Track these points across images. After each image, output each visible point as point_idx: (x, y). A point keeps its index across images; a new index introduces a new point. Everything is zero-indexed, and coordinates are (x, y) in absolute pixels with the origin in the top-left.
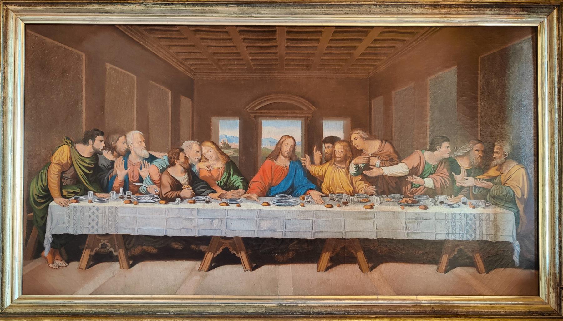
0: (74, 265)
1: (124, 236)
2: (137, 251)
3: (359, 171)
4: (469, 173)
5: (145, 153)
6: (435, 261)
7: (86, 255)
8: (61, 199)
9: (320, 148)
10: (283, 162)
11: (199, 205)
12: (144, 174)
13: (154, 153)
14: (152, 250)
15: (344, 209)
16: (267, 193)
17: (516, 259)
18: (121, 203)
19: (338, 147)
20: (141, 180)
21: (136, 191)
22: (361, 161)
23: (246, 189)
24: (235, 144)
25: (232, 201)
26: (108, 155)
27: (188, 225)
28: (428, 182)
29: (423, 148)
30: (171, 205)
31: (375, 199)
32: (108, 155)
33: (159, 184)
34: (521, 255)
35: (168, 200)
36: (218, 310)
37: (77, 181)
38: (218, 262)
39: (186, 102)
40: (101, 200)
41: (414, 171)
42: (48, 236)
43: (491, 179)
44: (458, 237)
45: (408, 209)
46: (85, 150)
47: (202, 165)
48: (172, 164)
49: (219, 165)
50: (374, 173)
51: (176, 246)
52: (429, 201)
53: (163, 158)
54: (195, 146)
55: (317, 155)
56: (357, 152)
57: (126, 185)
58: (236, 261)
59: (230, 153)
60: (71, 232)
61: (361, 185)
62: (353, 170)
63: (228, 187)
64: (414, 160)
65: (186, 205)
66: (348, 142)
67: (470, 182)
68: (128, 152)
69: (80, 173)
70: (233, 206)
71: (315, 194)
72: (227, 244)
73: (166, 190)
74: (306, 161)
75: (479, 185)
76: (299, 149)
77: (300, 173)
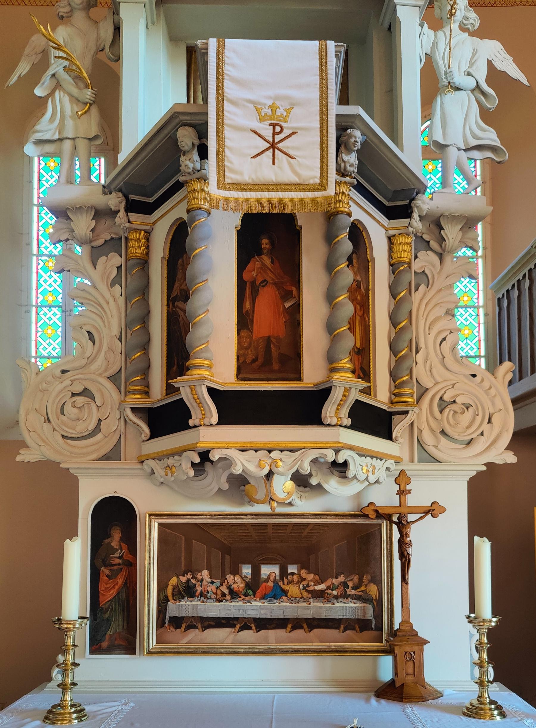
0: (178, 630)
1: (200, 617)
2: (206, 624)
3: (304, 588)
4: (353, 588)
5: (209, 580)
6: (338, 628)
7: (184, 626)
8: (173, 601)
9: (287, 578)
10: (270, 584)
11: (233, 603)
12: (209, 590)
13: (213, 580)
14: (213, 623)
15: (298, 605)
16: (263, 598)
17: (373, 627)
18: (199, 603)
19: (295, 577)
20: (208, 592)
21: (206, 597)
22: (305, 583)
23: (254, 596)
24: (250, 576)
25: (248, 601)
26: (194, 581)
27: (229, 612)
28: (335, 592)
29: (332, 578)
30: (221, 603)
31: (311, 600)
32: (194, 581)
33: (216, 594)
34: (375, 625)
35: (220, 601)
36: (242, 650)
37: (180, 593)
38: (242, 629)
39: (227, 557)
40: (190, 601)
41: (328, 588)
42: (167, 617)
43: (362, 591)
44: (348, 617)
45: (326, 605)
46: (183, 579)
47: (235, 585)
48: (222, 585)
49: (243, 585)
50: (311, 588)
51: (223, 622)
52: (335, 601)
53: (217, 582)
54: (232, 577)
55: (286, 581)
56: (303, 579)
57: (202, 594)
58: (251, 628)
59: (247, 580)
60: (177, 616)
61: (305, 594)
62: (301, 587)
63: (246, 595)
64: (328, 583)
65: (228, 603)
66: (299, 574)
67: (353, 592)
68: (202, 580)
69: (181, 589)
70: (248, 604)
71: (285, 598)
72: (246, 621)
73: (219, 596)
74: (281, 583)
75: (357, 594)
76: (278, 578)
77: (278, 589)
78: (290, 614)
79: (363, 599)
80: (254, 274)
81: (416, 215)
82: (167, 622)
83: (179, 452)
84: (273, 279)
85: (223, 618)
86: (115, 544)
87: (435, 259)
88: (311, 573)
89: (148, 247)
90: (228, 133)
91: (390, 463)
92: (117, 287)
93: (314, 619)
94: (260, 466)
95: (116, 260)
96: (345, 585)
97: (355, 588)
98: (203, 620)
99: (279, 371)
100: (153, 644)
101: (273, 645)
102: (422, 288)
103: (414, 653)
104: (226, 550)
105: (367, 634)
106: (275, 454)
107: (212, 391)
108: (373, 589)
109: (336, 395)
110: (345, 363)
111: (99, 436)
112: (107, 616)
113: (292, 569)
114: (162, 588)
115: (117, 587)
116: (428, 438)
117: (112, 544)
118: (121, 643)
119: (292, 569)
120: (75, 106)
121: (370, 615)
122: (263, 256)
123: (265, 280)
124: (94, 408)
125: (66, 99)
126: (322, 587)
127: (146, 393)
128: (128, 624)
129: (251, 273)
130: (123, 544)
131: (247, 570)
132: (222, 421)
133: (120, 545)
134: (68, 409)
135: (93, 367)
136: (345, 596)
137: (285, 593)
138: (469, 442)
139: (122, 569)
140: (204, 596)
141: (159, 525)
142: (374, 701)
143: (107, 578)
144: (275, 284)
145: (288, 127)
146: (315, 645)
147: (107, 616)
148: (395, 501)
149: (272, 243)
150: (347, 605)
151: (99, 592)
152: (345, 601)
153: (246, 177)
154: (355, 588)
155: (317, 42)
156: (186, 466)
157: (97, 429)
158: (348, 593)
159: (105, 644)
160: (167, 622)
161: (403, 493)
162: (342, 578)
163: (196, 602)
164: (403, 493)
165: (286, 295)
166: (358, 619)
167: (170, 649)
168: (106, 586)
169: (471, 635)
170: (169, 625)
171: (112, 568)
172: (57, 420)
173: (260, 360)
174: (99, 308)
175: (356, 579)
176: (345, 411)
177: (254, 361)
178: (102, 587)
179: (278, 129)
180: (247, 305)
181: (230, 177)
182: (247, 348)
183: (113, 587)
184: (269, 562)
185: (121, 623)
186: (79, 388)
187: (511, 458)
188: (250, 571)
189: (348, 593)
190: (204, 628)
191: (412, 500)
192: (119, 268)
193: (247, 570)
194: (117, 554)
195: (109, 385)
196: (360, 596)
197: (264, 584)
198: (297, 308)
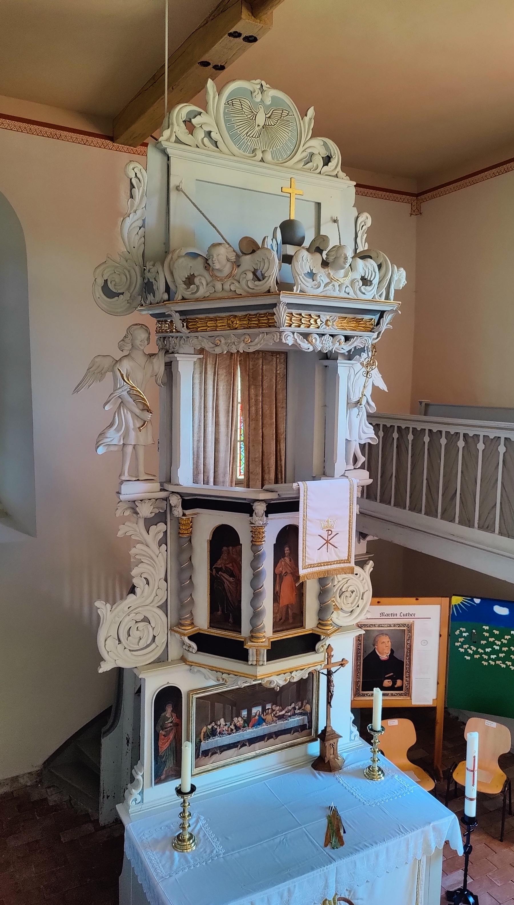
0: (207, 757)
1: (219, 746)
2: (222, 749)
3: (274, 715)
4: (298, 709)
5: (224, 724)
6: (290, 733)
7: (210, 754)
8: (204, 741)
9: (265, 712)
10: (257, 717)
11: (237, 734)
12: (224, 729)
13: (227, 723)
14: (226, 748)
15: (271, 725)
16: (253, 726)
17: (307, 727)
18: (219, 738)
19: (270, 710)
20: (223, 731)
21: (223, 734)
22: (274, 713)
23: (248, 727)
24: (246, 716)
25: (245, 730)
26: (216, 727)
27: (234, 739)
28: (289, 714)
29: (288, 706)
30: (231, 735)
31: (278, 721)
32: (216, 727)
33: (228, 731)
34: (308, 726)
35: (230, 734)
37: (208, 735)
38: (241, 747)
39: (234, 708)
40: (214, 739)
41: (286, 712)
42: (201, 751)
43: (303, 710)
44: (295, 726)
45: (285, 722)
46: (210, 727)
47: (238, 723)
48: (231, 725)
49: (242, 722)
50: (278, 715)
51: (231, 745)
52: (290, 718)
53: (228, 723)
54: (236, 719)
55: (265, 714)
56: (273, 711)
57: (220, 733)
58: (246, 745)
59: (245, 718)
60: (206, 749)
61: (275, 719)
62: (273, 715)
63: (244, 727)
64: (286, 709)
65: (234, 734)
66: (272, 708)
67: (299, 711)
68: (220, 724)
69: (208, 733)
70: (245, 732)
71: (264, 724)
72: (243, 741)
73: (229, 732)
74: (262, 716)
75: (300, 711)
76: (261, 713)
77: (261, 719)
78: (266, 732)
79: (304, 714)
80: (281, 569)
82: (200, 754)
84: (290, 571)
85: (231, 744)
86: (168, 715)
88: (278, 706)
90: (308, 538)
92: (164, 546)
93: (278, 731)
95: (162, 526)
96: (294, 708)
97: (299, 709)
98: (220, 747)
99: (292, 623)
103: (334, 743)
104: (234, 704)
112: (164, 759)
113: (268, 706)
115: (169, 741)
117: (167, 715)
118: (172, 773)
119: (268, 706)
120: (136, 421)
121: (306, 722)
122: (286, 558)
123: (286, 572)
124: (151, 629)
125: (129, 416)
128: (176, 761)
129: (279, 569)
130: (173, 714)
131: (244, 713)
133: (172, 715)
134: (133, 632)
136: (294, 714)
137: (264, 720)
139: (172, 729)
143: (164, 737)
144: (291, 573)
147: (164, 759)
149: (290, 549)
150: (295, 719)
151: (158, 746)
152: (294, 717)
154: (299, 709)
158: (296, 712)
159: (163, 777)
160: (200, 754)
166: (300, 726)
167: (203, 769)
168: (163, 742)
169: (351, 718)
170: (202, 756)
171: (166, 730)
172: (126, 641)
173: (284, 618)
174: (152, 561)
175: (300, 704)
177: (280, 620)
178: (160, 743)
179: (330, 532)
180: (277, 588)
182: (277, 614)
183: (167, 741)
184: (256, 705)
185: (172, 761)
186: (140, 617)
188: (246, 713)
189: (296, 712)
192: (165, 533)
193: (244, 713)
194: (170, 721)
195: (160, 613)
196: (302, 712)
197: (254, 718)
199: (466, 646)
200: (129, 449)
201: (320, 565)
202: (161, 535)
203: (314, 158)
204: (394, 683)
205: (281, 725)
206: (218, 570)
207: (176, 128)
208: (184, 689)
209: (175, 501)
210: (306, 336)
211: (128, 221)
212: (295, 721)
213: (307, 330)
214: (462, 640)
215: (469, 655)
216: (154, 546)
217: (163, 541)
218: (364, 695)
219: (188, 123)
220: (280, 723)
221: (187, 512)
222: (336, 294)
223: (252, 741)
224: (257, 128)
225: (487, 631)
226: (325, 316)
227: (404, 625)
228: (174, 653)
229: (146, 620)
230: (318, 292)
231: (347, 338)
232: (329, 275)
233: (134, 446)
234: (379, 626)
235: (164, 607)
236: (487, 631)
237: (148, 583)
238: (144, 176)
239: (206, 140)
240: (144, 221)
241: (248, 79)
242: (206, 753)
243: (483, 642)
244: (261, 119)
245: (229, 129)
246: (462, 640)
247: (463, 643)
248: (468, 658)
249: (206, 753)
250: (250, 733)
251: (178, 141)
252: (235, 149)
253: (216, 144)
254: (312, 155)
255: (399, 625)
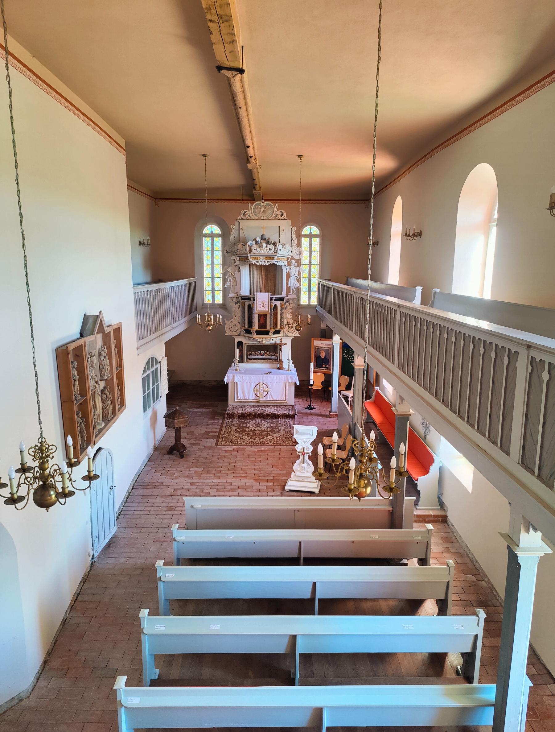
16: (261, 356)
56: (267, 353)
78: (265, 358)
81: (284, 300)
83: (251, 337)
87: (289, 304)
89: (244, 304)
90: (258, 305)
91: (280, 337)
94: (261, 340)
95: (239, 304)
96: (273, 354)
100: (246, 362)
101: (263, 362)
102: (286, 309)
104: (256, 349)
105: (276, 361)
106: (263, 339)
107: (255, 331)
108: (277, 355)
109: (271, 332)
110: (272, 328)
111: (237, 331)
114: (247, 354)
116: (286, 333)
119: (266, 352)
126: (270, 354)
127: (245, 327)
131: (259, 352)
132: (256, 335)
134: (232, 327)
135: (236, 321)
136: (273, 355)
137: (265, 355)
138: (293, 333)
140: (253, 355)
141: (247, 345)
142: (276, 369)
145: (265, 304)
146: (269, 362)
148: (280, 342)
153: (260, 310)
155: (268, 293)
156: (251, 339)
157: (237, 330)
161: (281, 342)
162: (273, 353)
163: (252, 356)
164: (281, 342)
165: (264, 318)
175: (275, 353)
176: (272, 333)
180: (260, 319)
181: (258, 310)
187: (299, 335)
190: (253, 360)
191: (282, 343)
192: (240, 306)
195: (239, 324)
198: (266, 319)
199: (346, 355)
200: (231, 286)
201: (261, 311)
202: (239, 306)
203: (278, 216)
204: (326, 366)
205: (269, 357)
206: (249, 314)
207: (241, 216)
208: (244, 342)
209: (240, 298)
210: (257, 262)
211: (231, 237)
212: (273, 357)
213: (257, 260)
214: (345, 353)
215: (347, 358)
216: (237, 308)
217: (239, 308)
218: (317, 369)
219: (244, 214)
220: (269, 356)
221: (243, 301)
222: (262, 253)
223: (261, 359)
224: (261, 212)
225: (351, 350)
226: (261, 257)
227: (329, 348)
228: (242, 334)
229: (235, 325)
230: (258, 253)
231: (268, 262)
232: (260, 249)
233: (233, 286)
234: (321, 347)
235: (239, 323)
236: (351, 350)
237: (236, 317)
238: (234, 227)
239: (248, 217)
240: (235, 236)
241: (259, 201)
242: (249, 359)
243: (350, 354)
244: (263, 209)
245: (254, 213)
246: (345, 353)
247: (345, 354)
248: (346, 359)
249: (249, 359)
250: (260, 357)
251: (242, 219)
252: (256, 218)
253: (251, 217)
254: (277, 215)
255: (327, 348)
